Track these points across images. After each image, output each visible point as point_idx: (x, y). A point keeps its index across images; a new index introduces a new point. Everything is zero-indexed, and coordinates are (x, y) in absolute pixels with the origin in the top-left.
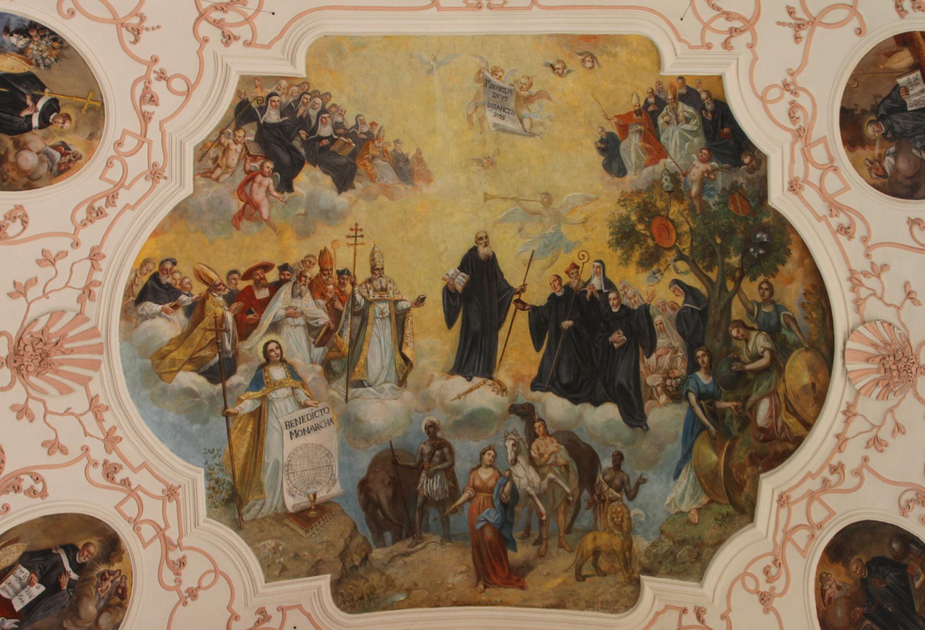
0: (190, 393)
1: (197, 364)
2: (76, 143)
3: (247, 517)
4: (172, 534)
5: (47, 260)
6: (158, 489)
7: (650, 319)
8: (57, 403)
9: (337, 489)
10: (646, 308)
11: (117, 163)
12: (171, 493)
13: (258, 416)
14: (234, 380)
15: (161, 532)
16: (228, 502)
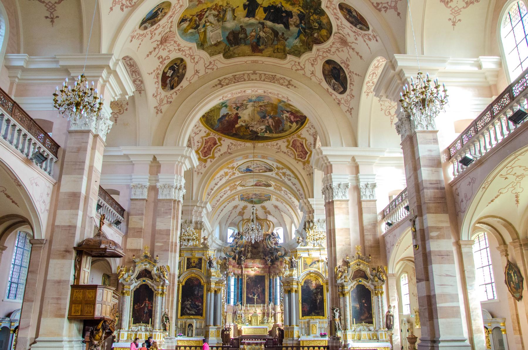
0: (191, 33)
1: (192, 28)
2: (166, 11)
3: (205, 47)
4: (192, 54)
5: (163, 27)
6: (188, 49)
7: (292, 14)
8: (168, 45)
9: (222, 39)
10: (291, 12)
11: (174, 9)
12: (190, 48)
13: (205, 32)
14: (199, 28)
15: (190, 55)
16: (201, 46)
